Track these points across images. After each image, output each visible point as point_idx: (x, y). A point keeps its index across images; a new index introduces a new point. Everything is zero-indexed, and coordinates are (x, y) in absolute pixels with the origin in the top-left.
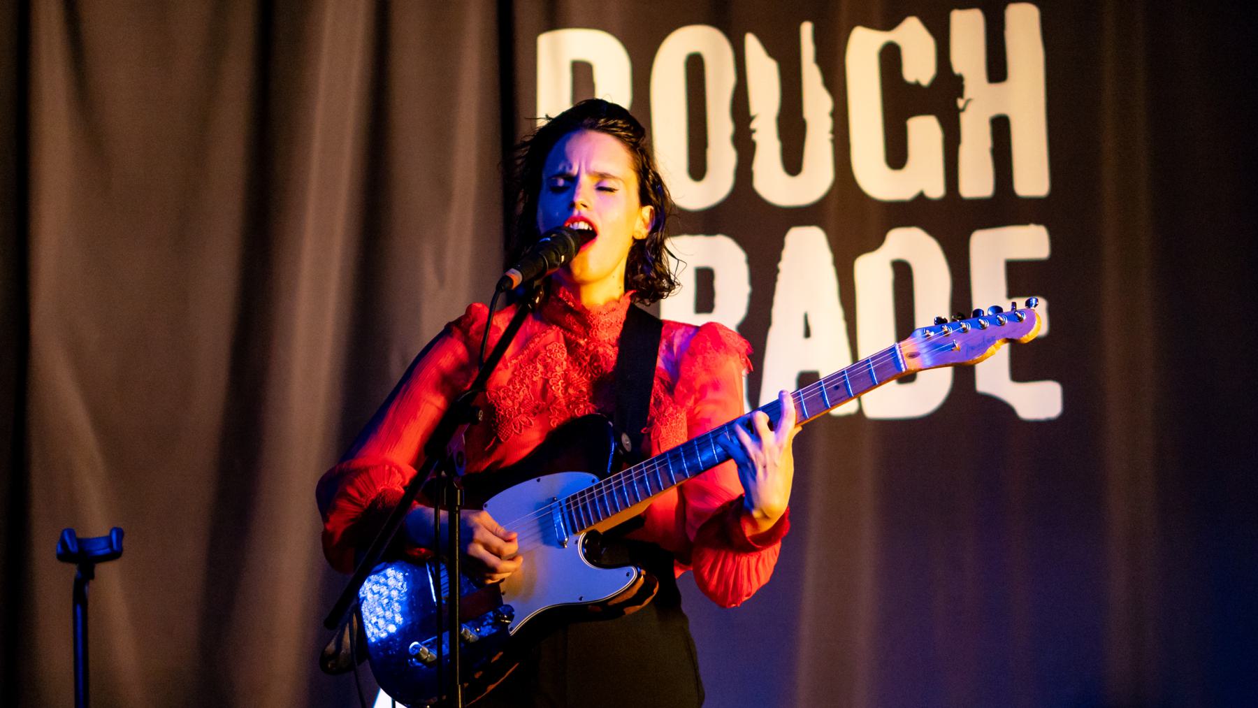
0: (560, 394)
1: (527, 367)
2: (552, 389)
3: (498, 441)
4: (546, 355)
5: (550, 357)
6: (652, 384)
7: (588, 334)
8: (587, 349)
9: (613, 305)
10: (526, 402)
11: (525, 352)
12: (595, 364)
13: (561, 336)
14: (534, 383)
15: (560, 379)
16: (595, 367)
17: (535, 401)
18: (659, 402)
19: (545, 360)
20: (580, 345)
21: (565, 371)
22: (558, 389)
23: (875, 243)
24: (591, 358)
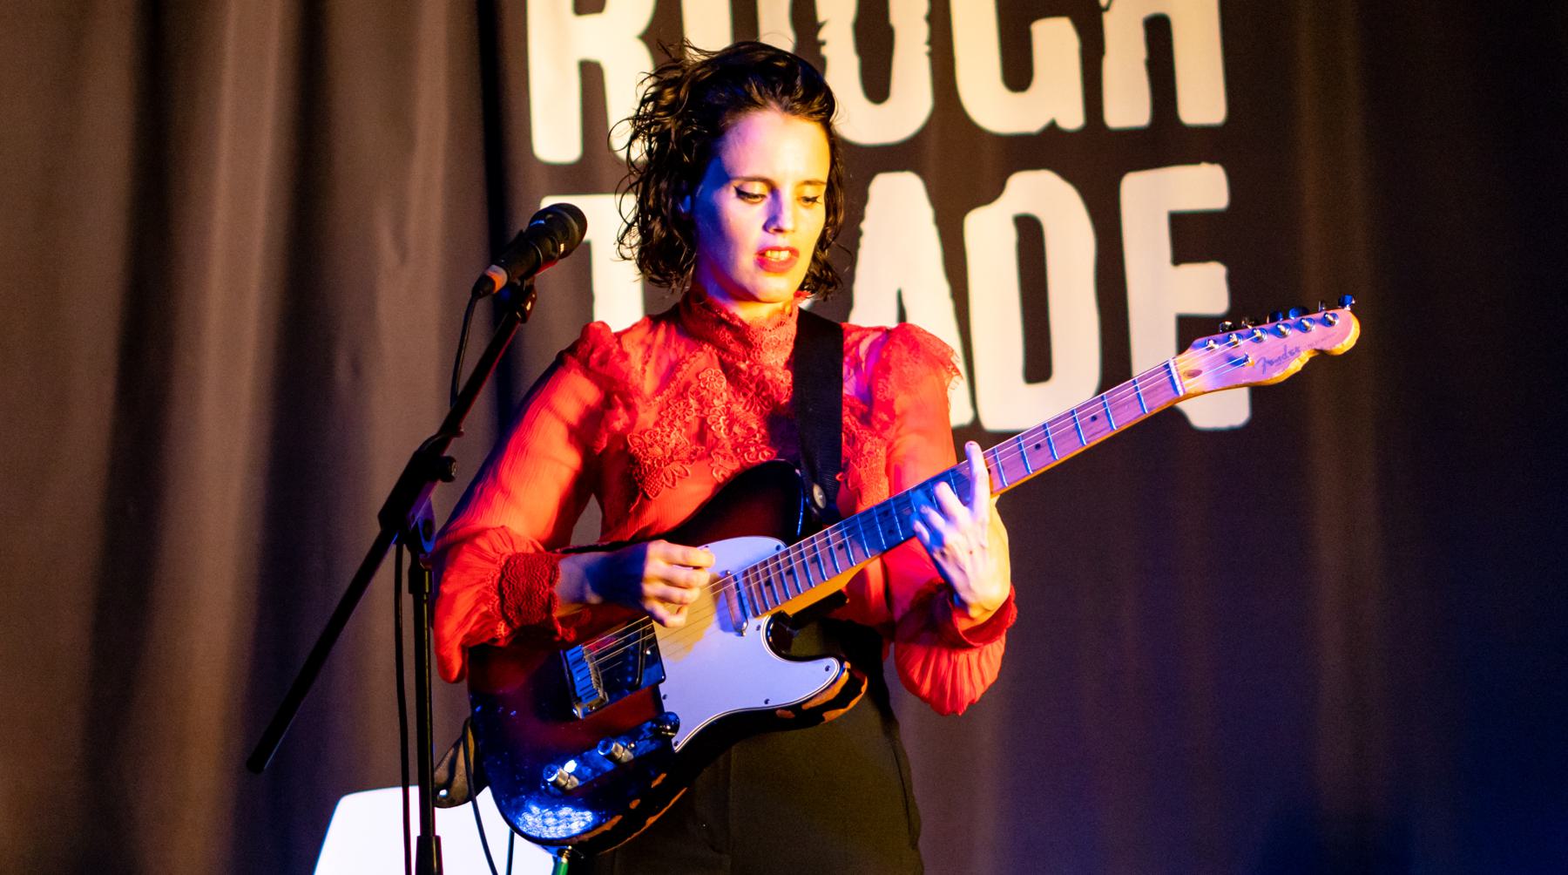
0: (722, 434)
1: (677, 405)
2: (712, 430)
3: (645, 496)
4: (699, 386)
5: (705, 388)
6: (840, 420)
7: (749, 355)
8: (750, 374)
9: (778, 318)
10: (679, 448)
11: (672, 385)
12: (764, 394)
13: (716, 358)
14: (687, 425)
15: (722, 415)
16: (763, 397)
17: (691, 446)
18: (853, 439)
19: (699, 393)
20: (741, 370)
21: (727, 403)
22: (720, 429)
23: (992, 192)
24: (757, 386)
